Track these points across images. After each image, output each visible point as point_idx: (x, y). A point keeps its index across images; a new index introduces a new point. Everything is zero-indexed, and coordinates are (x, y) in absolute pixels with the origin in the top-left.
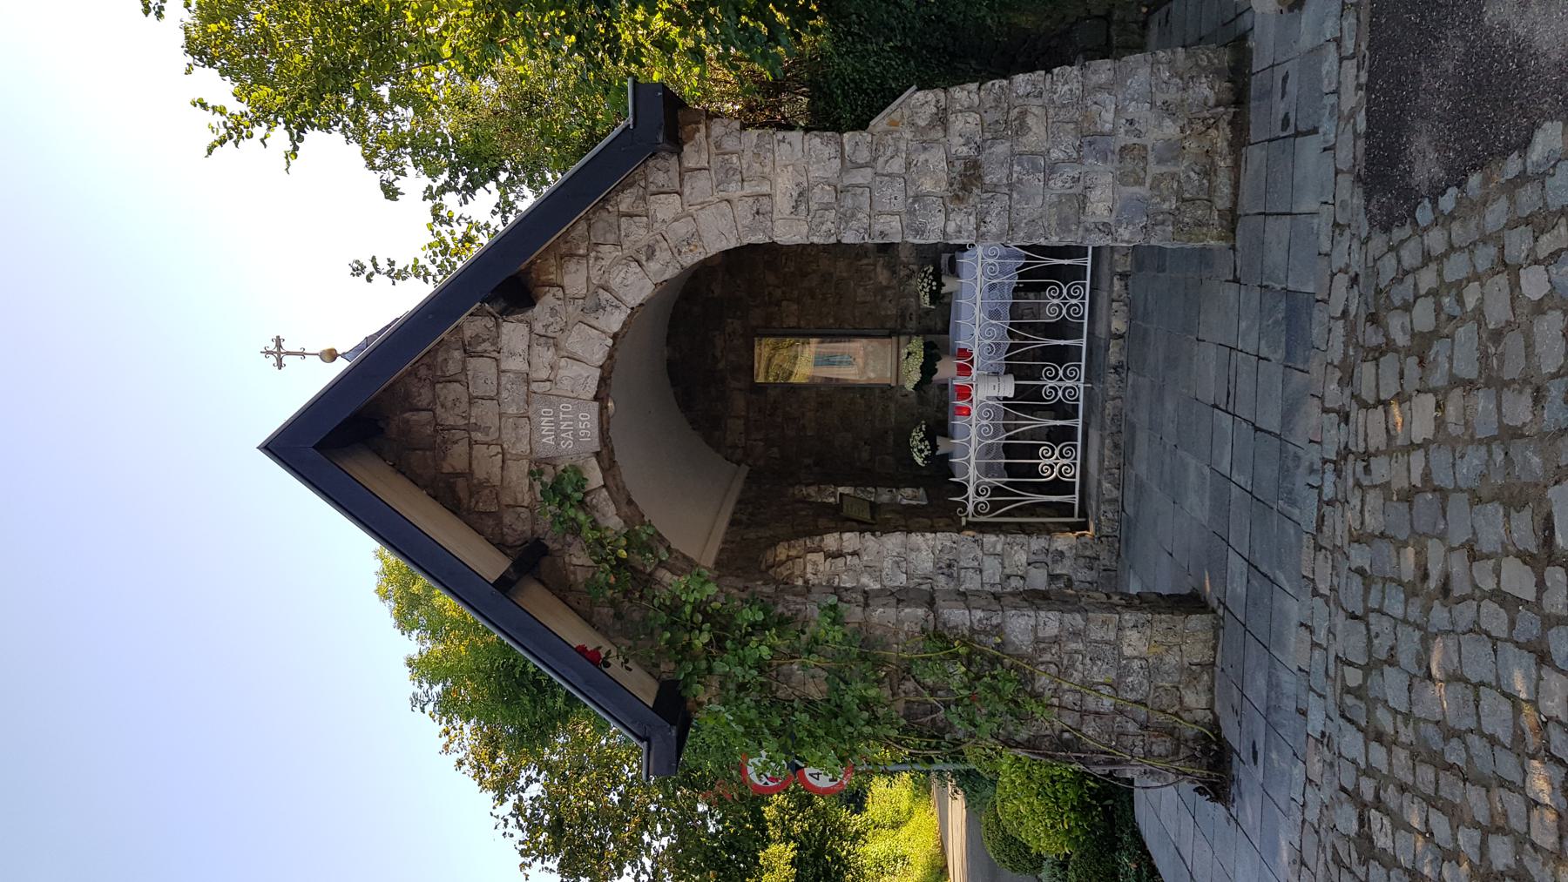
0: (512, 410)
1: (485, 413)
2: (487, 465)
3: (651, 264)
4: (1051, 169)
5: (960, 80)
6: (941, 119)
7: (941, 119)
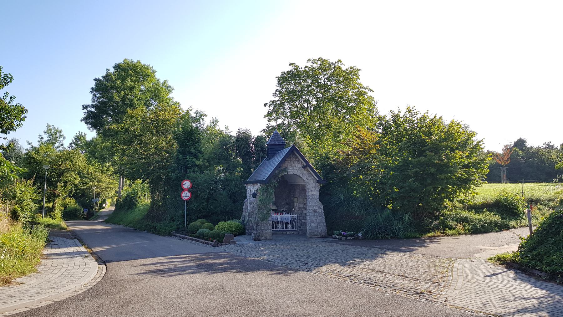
1: (292, 162)
2: (287, 162)
6: (320, 208)
7: (320, 208)
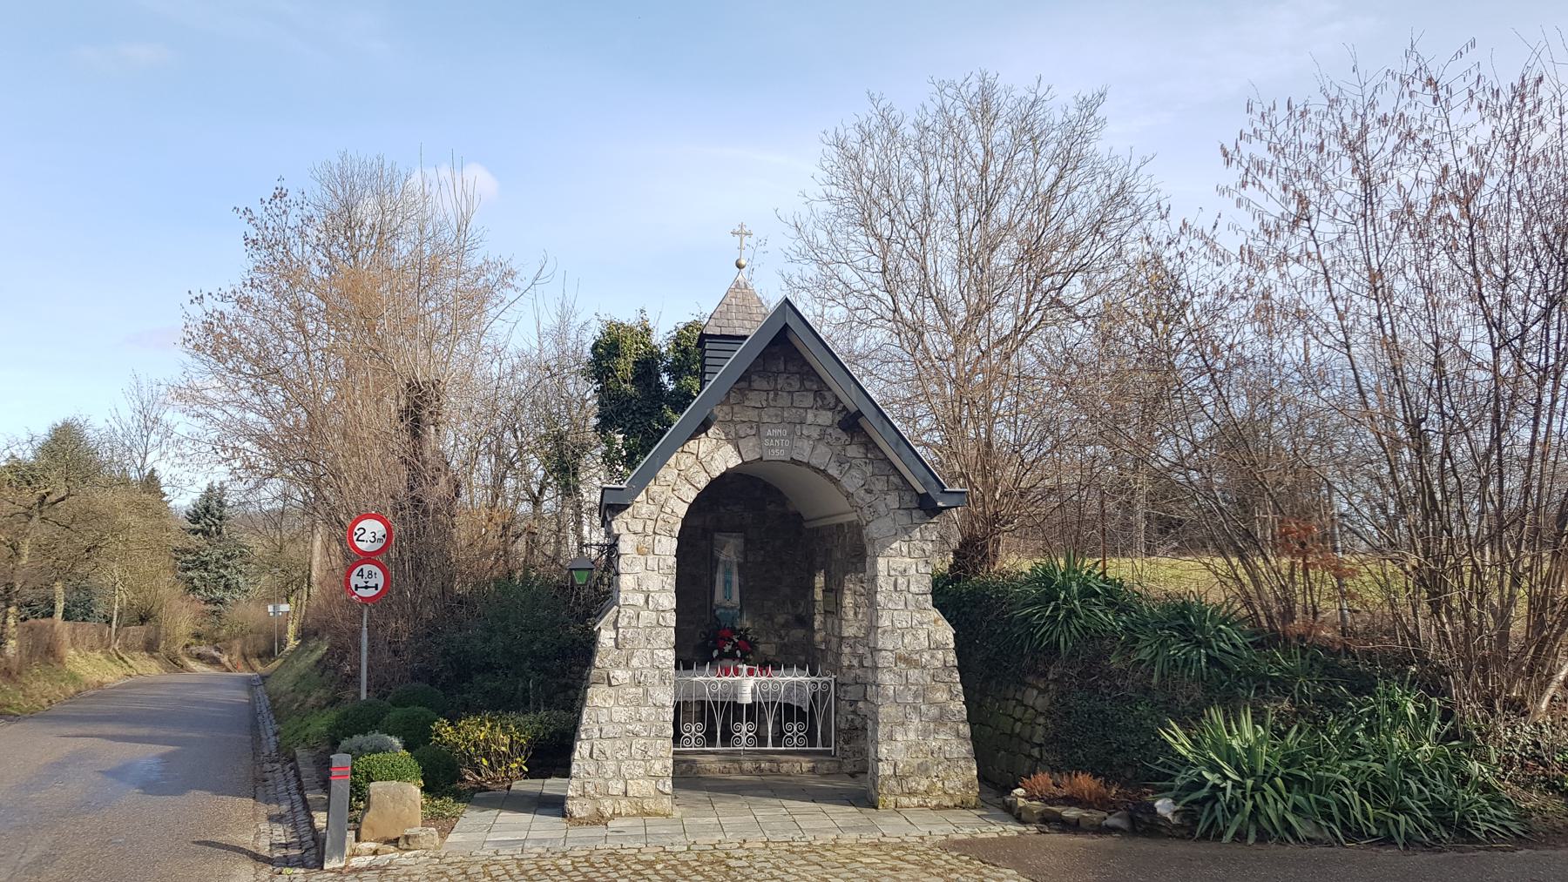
1: (784, 400)
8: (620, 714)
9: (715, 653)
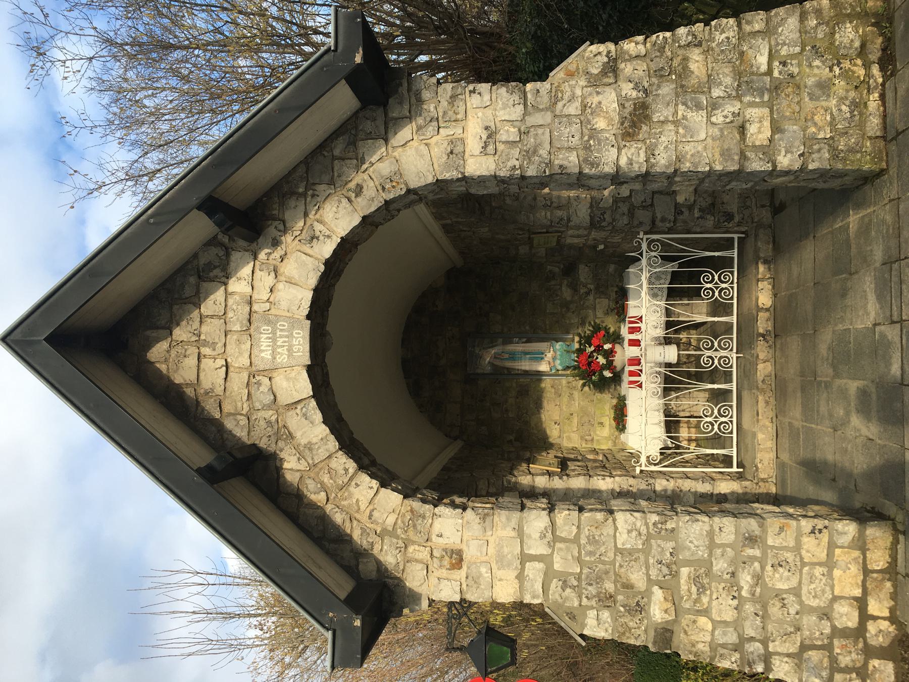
0: (237, 327)
3: (359, 199)
4: (714, 106)
5: (626, 34)
6: (612, 68)
7: (612, 68)
8: (723, 607)
9: (607, 374)
